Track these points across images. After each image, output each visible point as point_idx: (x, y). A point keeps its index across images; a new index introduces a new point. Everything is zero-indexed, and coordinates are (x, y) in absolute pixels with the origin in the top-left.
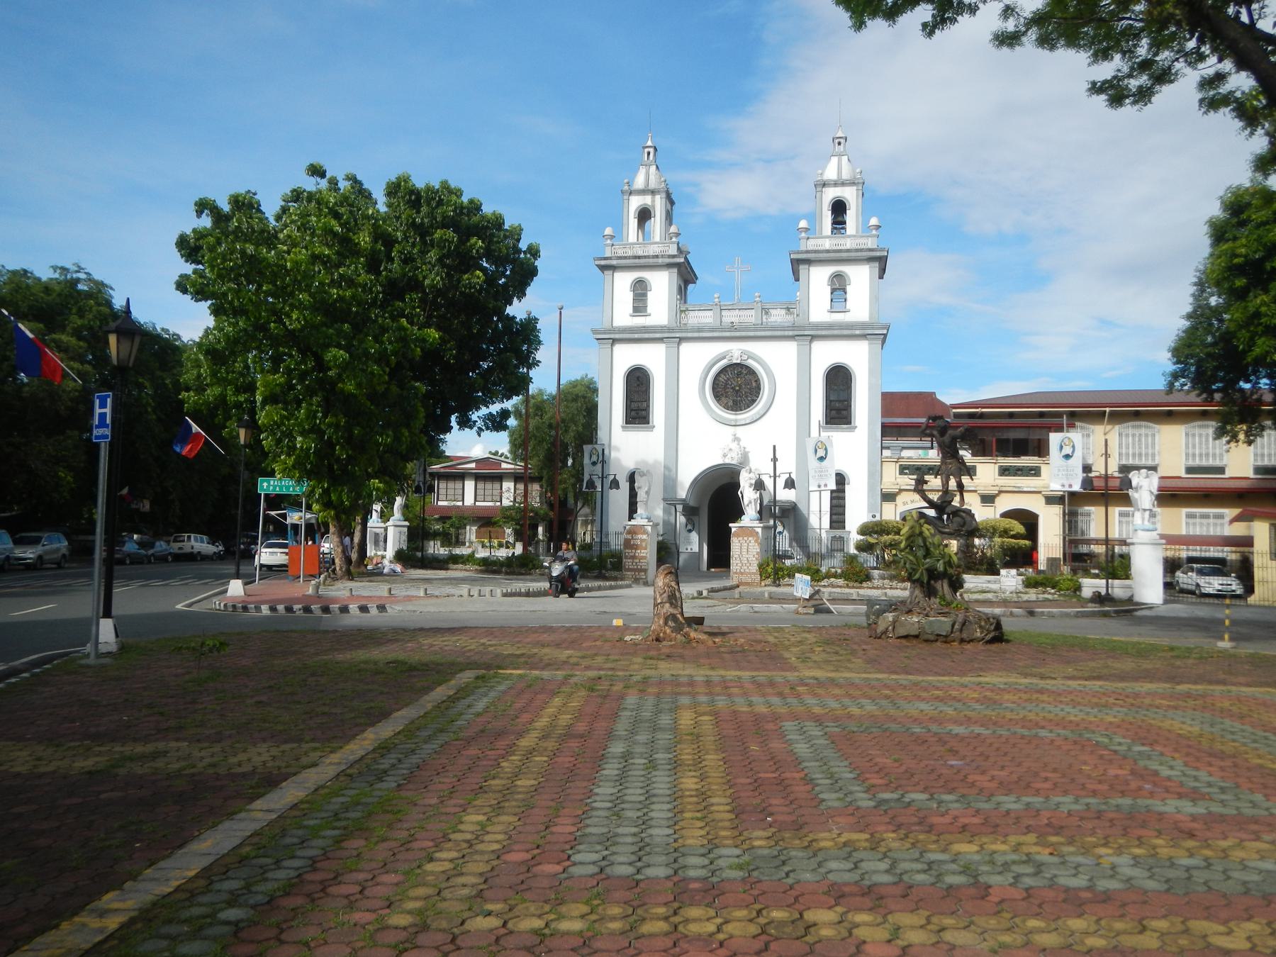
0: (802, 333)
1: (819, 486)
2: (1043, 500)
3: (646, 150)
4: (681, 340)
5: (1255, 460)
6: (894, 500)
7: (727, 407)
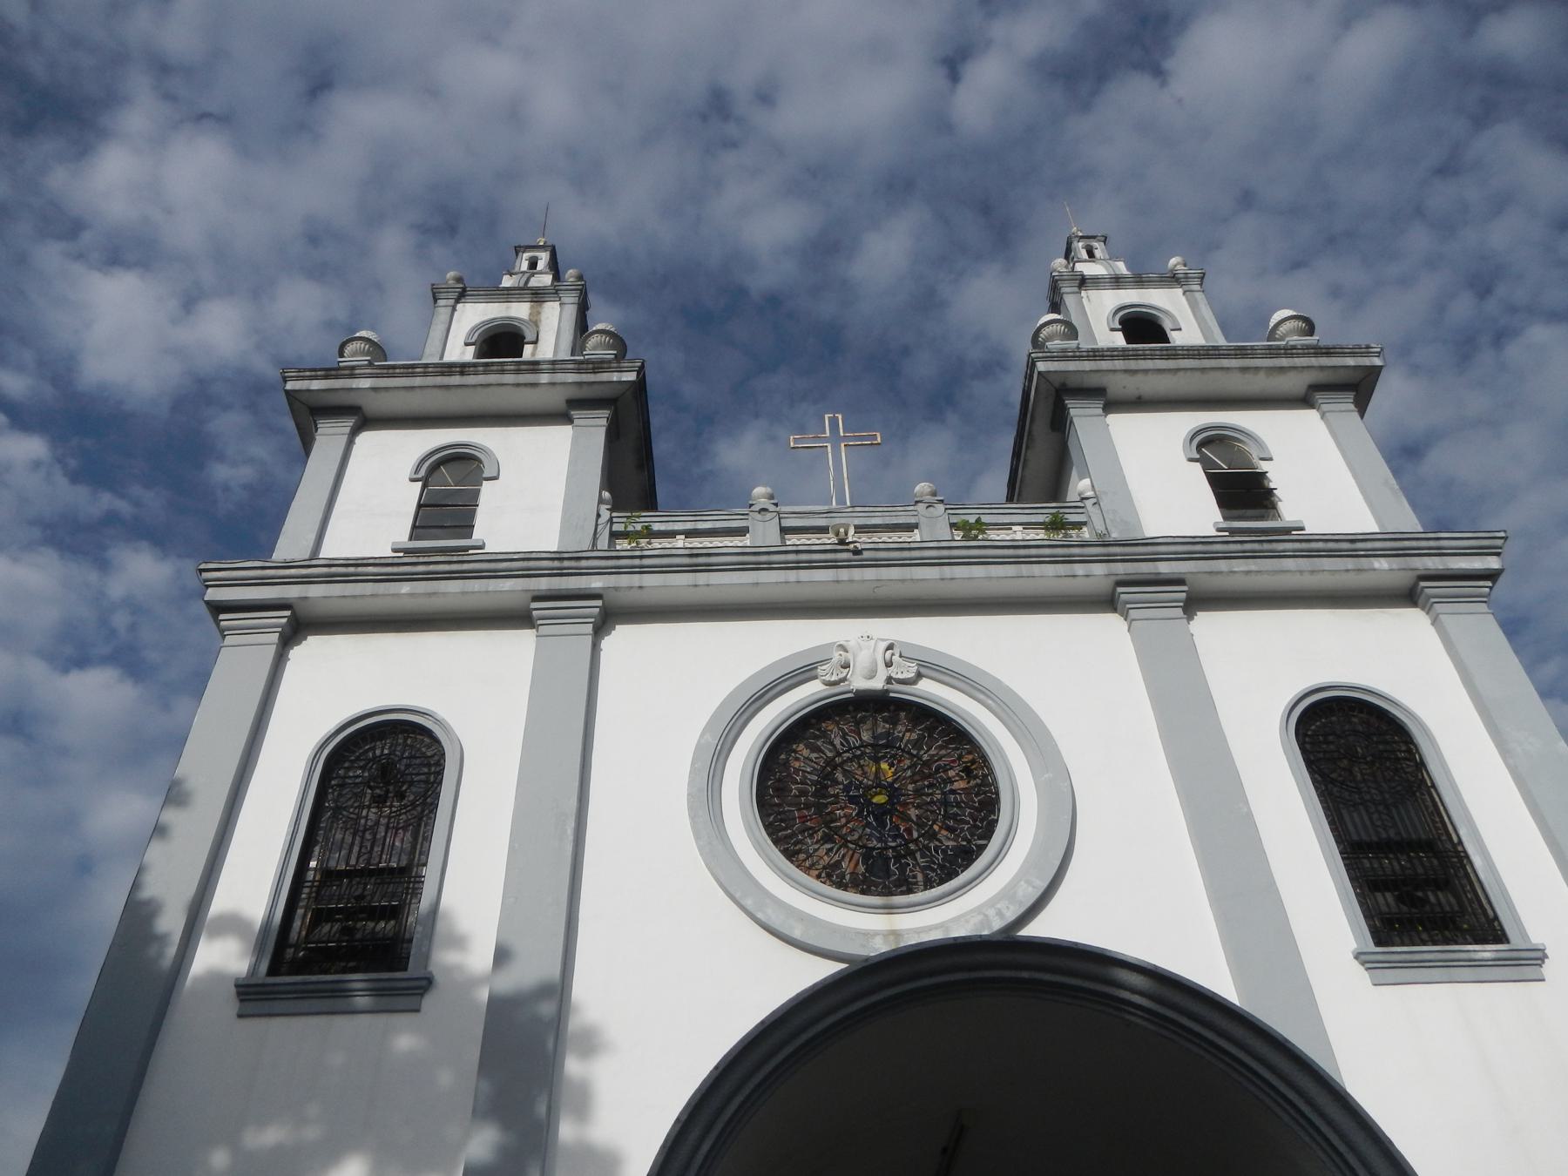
0: (1145, 568)
3: (526, 255)
4: (610, 616)
7: (832, 875)
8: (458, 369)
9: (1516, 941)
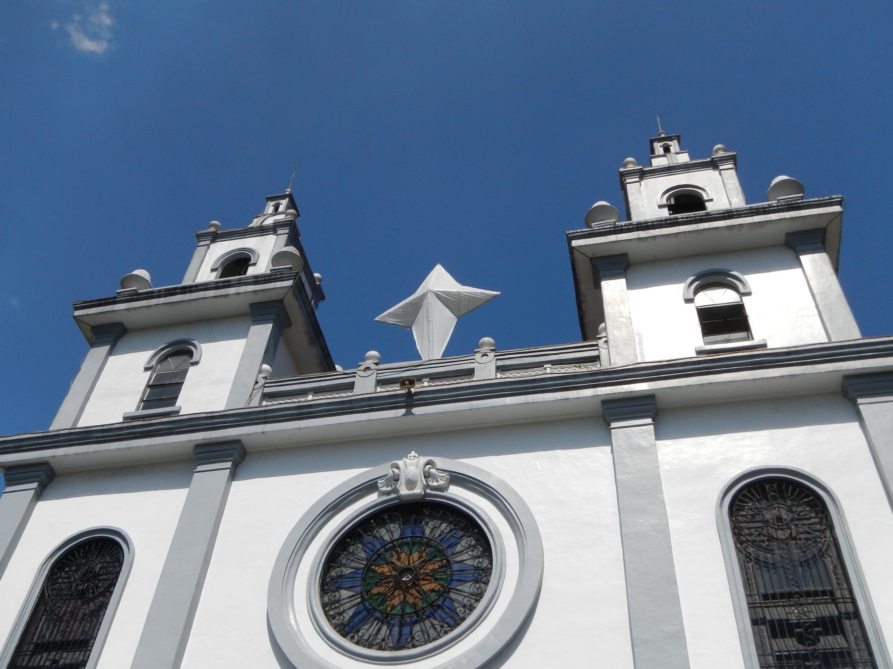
3: (273, 203)
8: (179, 291)
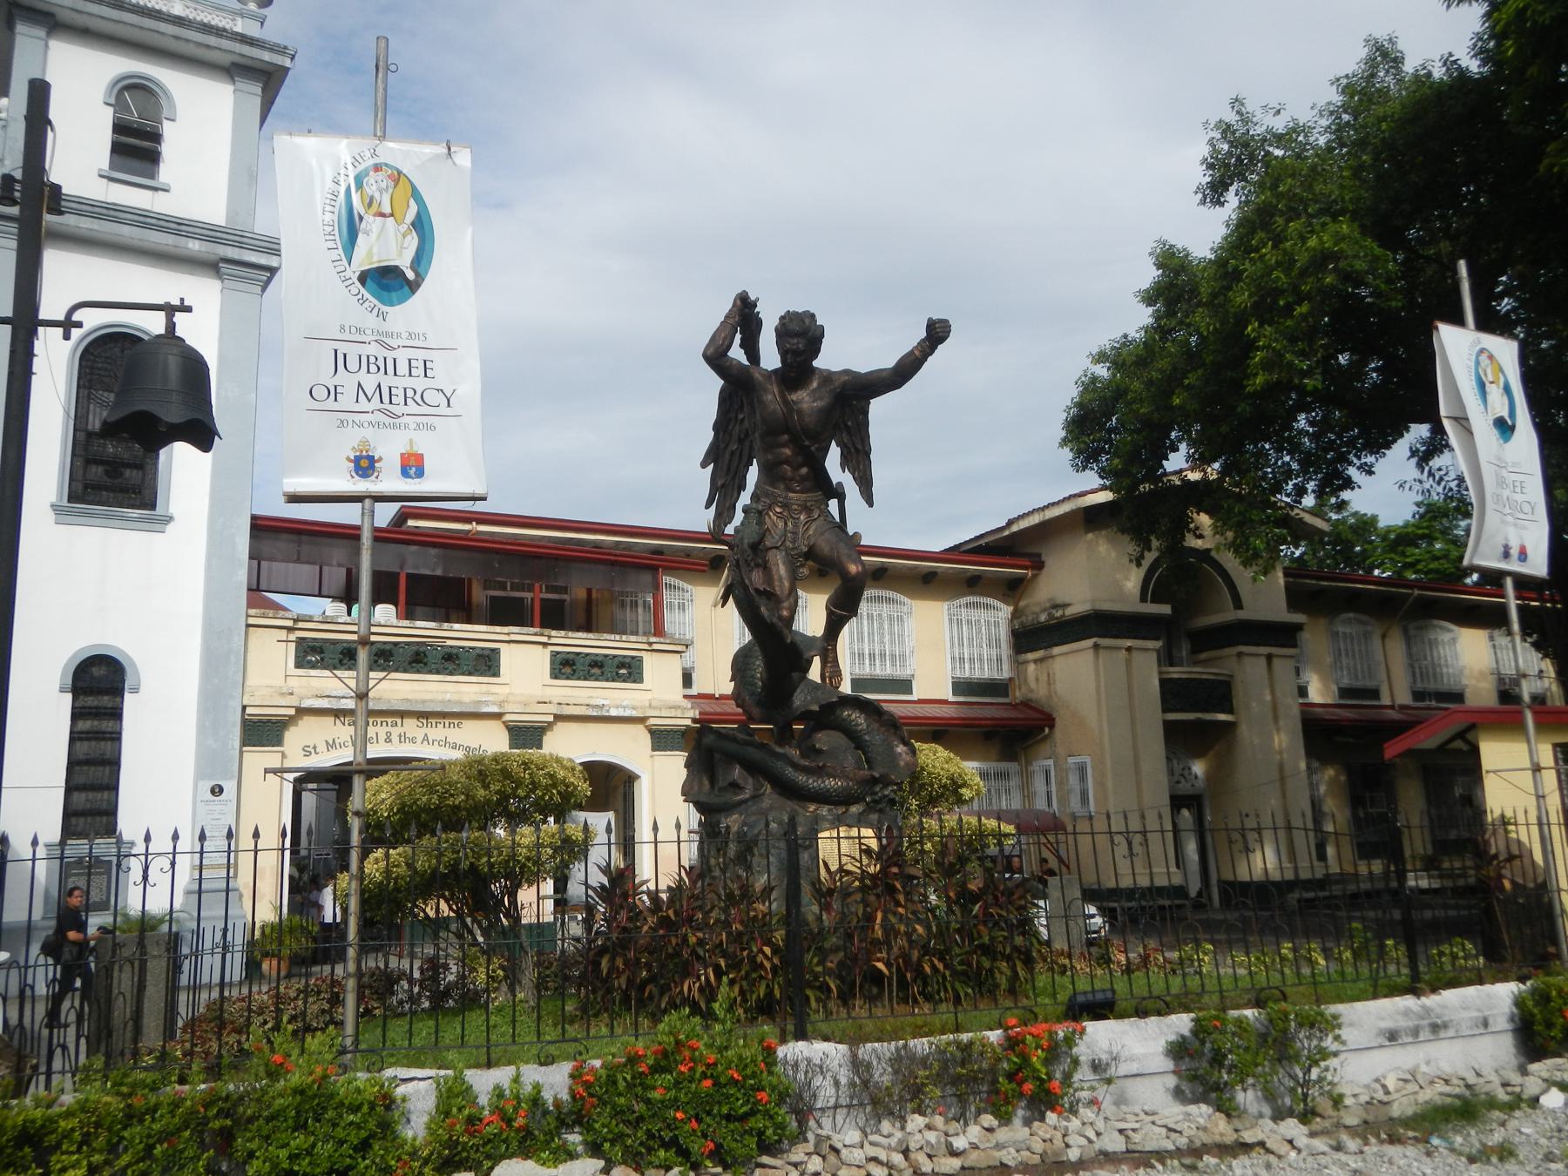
1: (365, 465)
2: (646, 740)
5: (953, 669)
6: (277, 740)
9: (159, 510)
